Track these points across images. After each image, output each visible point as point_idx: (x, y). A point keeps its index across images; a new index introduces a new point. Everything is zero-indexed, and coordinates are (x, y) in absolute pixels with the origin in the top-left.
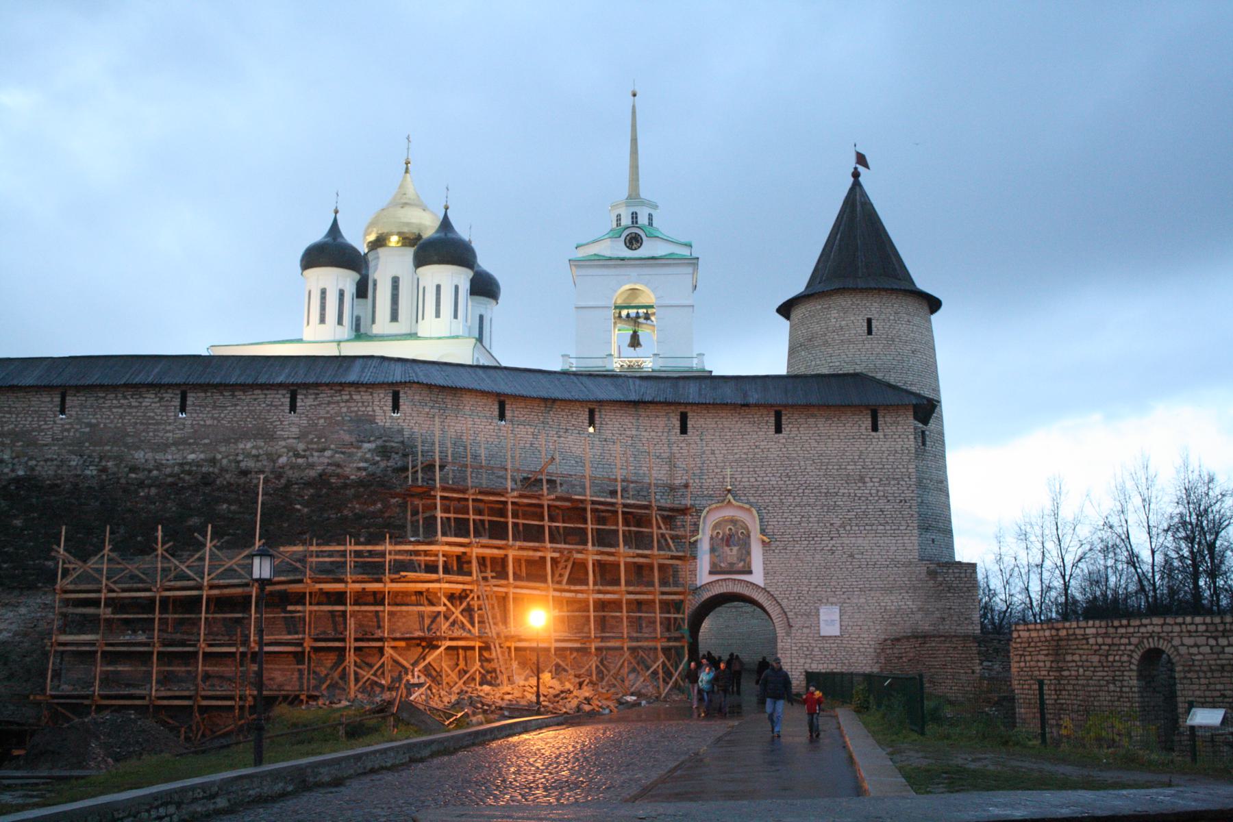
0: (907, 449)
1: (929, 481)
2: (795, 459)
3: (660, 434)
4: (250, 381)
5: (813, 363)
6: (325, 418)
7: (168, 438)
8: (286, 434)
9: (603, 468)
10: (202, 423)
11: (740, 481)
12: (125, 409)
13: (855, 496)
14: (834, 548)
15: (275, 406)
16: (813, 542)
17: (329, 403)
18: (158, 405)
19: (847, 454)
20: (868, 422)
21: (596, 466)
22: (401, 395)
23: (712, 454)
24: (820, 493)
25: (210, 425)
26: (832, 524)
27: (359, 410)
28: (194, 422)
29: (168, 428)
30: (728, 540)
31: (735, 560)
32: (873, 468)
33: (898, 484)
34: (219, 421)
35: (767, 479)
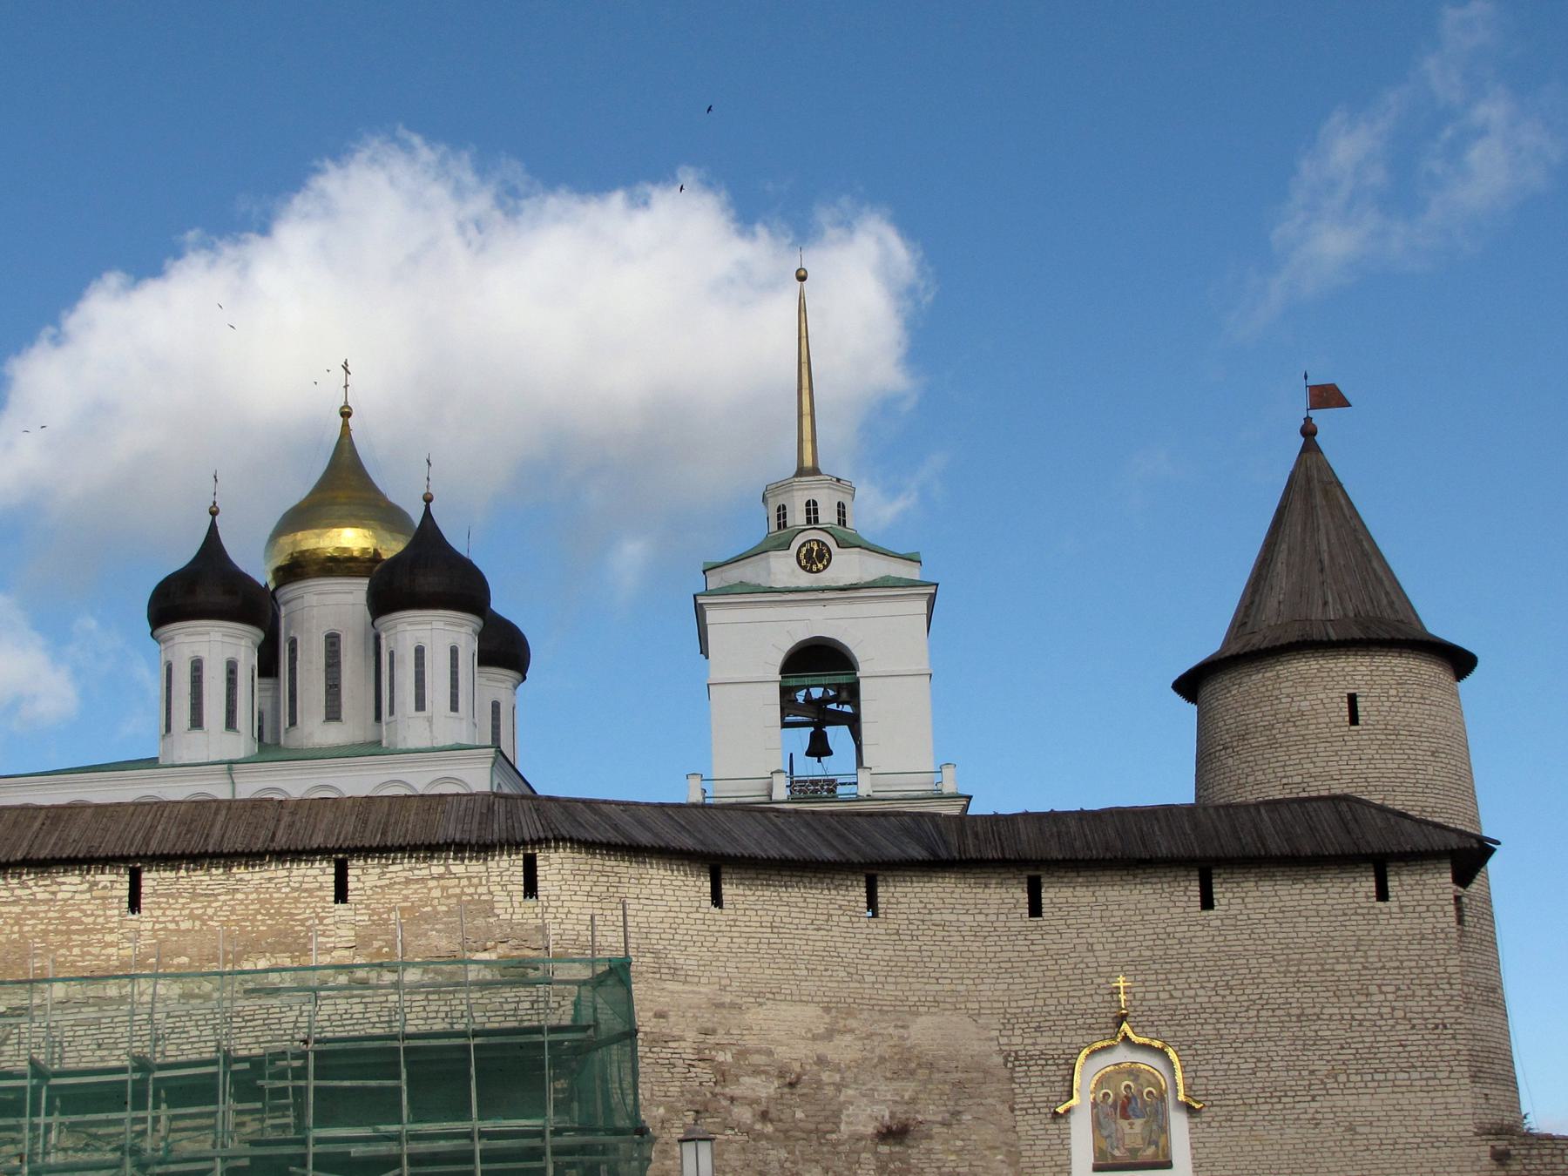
0: (1442, 929)
1: (1472, 989)
2: (1239, 955)
3: (993, 918)
4: (258, 846)
5: (1251, 779)
6: (402, 910)
7: (109, 956)
8: (330, 942)
9: (896, 983)
10: (172, 926)
11: (1144, 999)
12: (25, 906)
15: (306, 890)
16: (1280, 1106)
17: (408, 881)
18: (88, 896)
19: (1335, 943)
20: (1369, 885)
21: (883, 979)
22: (538, 863)
23: (1089, 951)
24: (1289, 1015)
25: (189, 931)
26: (1312, 1072)
27: (463, 893)
28: (157, 926)
29: (108, 938)
30: (1126, 1107)
31: (1138, 1143)
34: (204, 923)
35: (1192, 993)
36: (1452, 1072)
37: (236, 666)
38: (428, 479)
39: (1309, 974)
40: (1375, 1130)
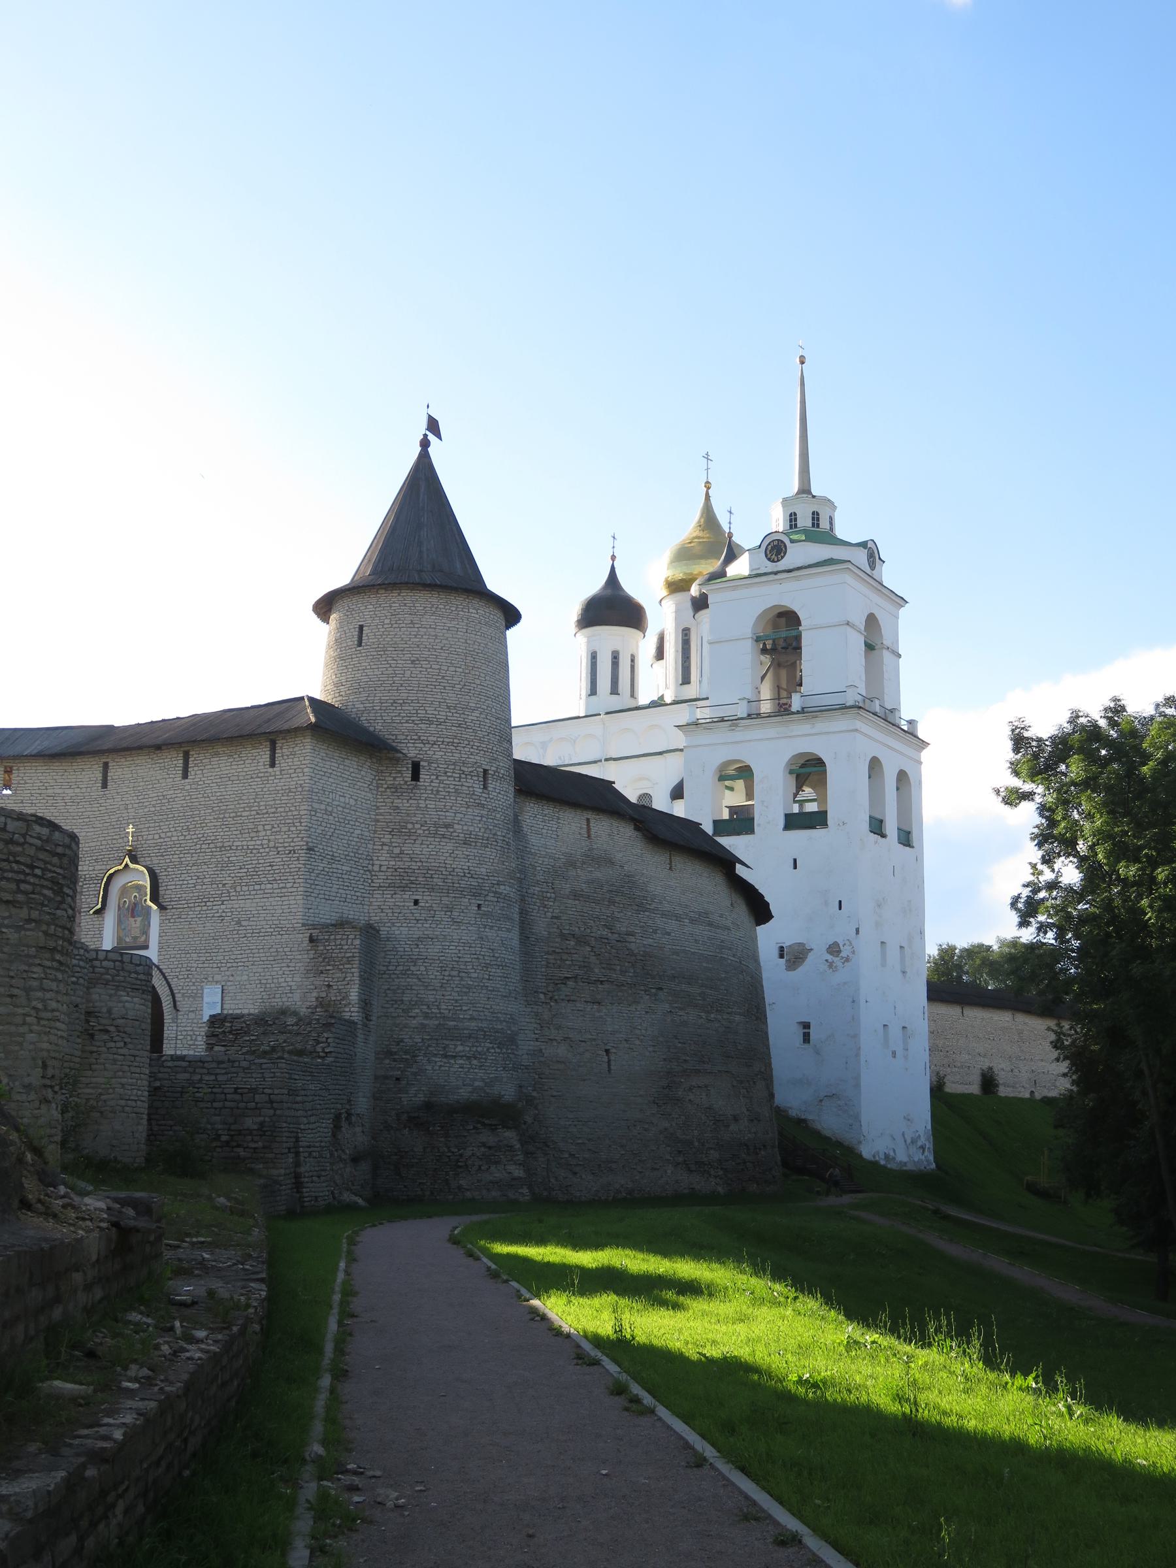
0: (301, 784)
13: (248, 849)
14: (224, 914)
20: (266, 757)
26: (224, 885)
32: (267, 813)
33: (289, 831)
36: (295, 883)
37: (618, 654)
38: (730, 523)
39: (229, 819)
40: (251, 923)
